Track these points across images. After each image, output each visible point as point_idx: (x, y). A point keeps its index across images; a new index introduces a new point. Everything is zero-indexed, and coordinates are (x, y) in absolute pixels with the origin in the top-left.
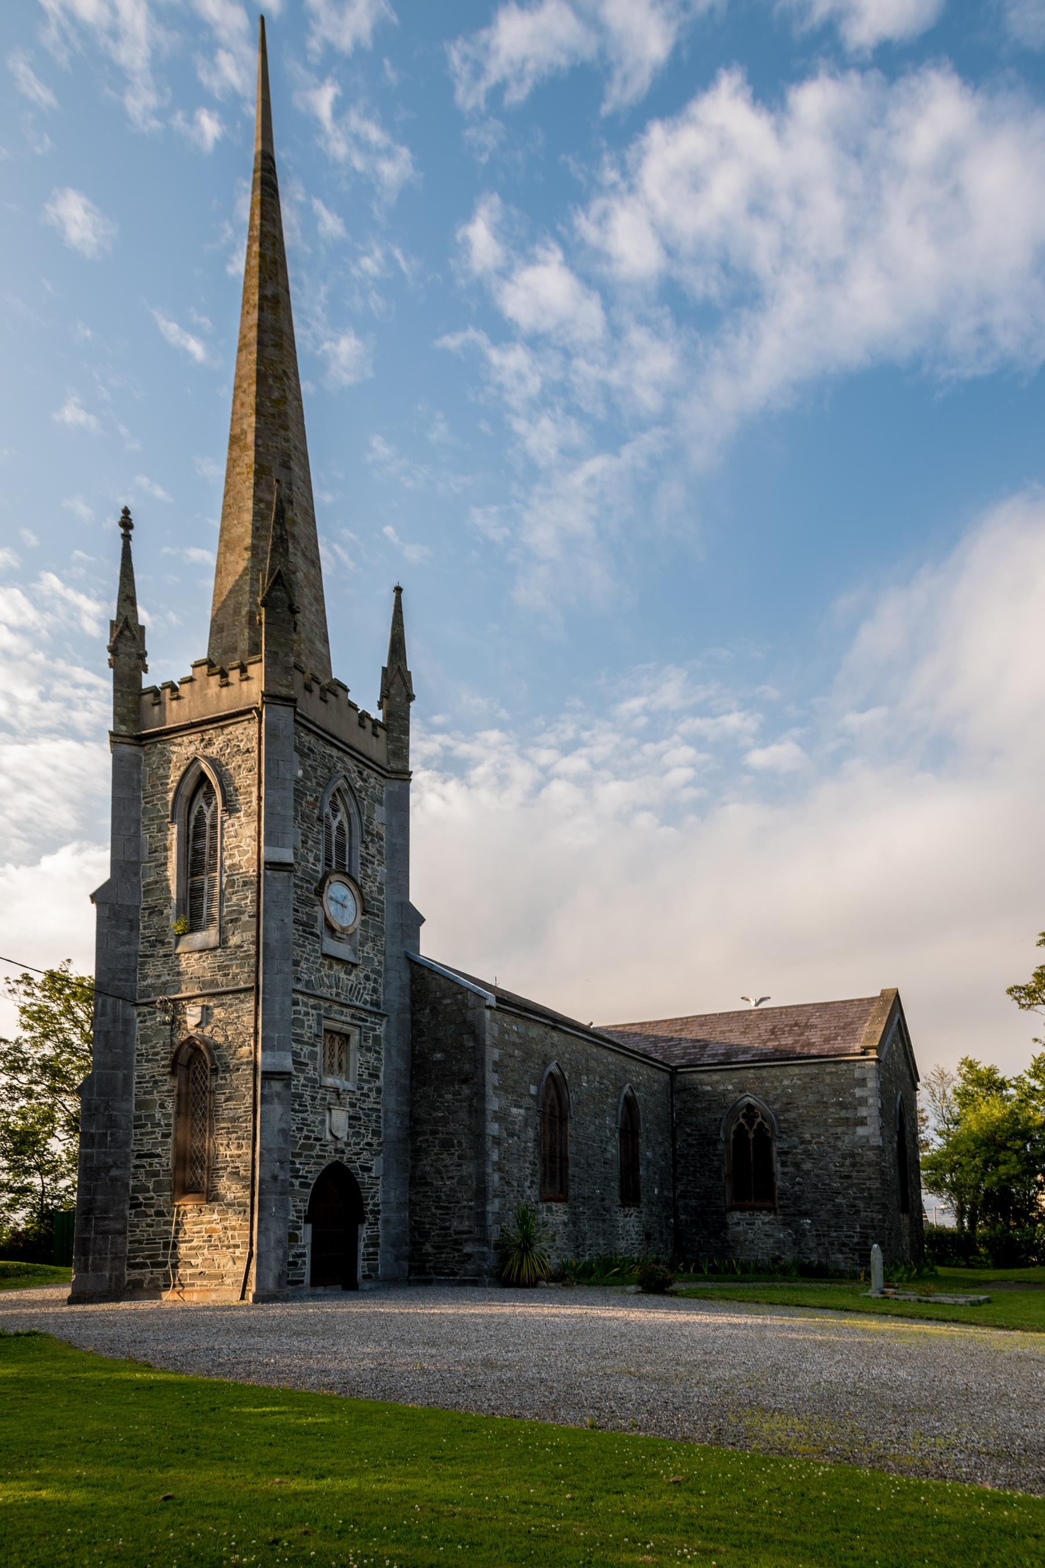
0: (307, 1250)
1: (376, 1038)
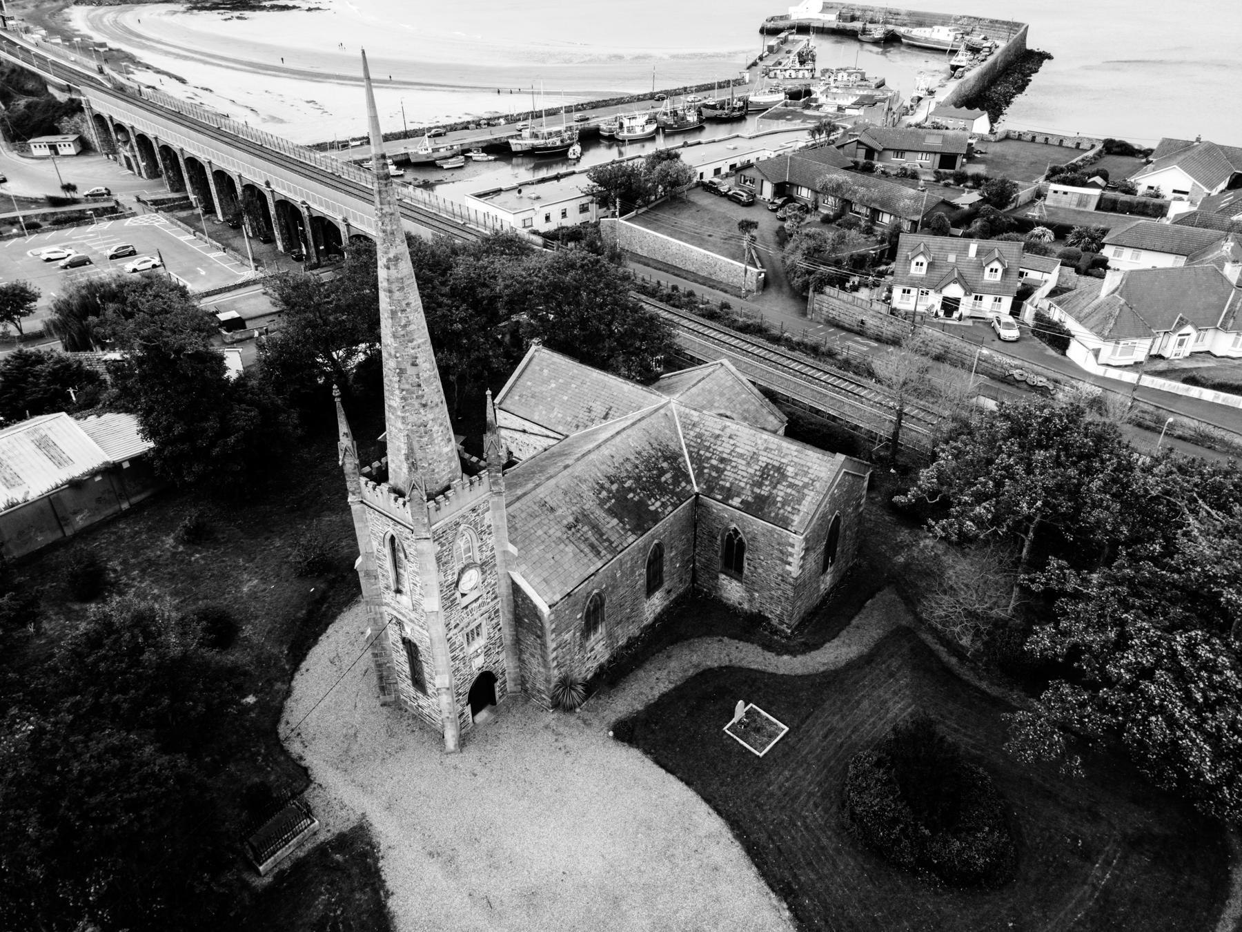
1: (497, 611)
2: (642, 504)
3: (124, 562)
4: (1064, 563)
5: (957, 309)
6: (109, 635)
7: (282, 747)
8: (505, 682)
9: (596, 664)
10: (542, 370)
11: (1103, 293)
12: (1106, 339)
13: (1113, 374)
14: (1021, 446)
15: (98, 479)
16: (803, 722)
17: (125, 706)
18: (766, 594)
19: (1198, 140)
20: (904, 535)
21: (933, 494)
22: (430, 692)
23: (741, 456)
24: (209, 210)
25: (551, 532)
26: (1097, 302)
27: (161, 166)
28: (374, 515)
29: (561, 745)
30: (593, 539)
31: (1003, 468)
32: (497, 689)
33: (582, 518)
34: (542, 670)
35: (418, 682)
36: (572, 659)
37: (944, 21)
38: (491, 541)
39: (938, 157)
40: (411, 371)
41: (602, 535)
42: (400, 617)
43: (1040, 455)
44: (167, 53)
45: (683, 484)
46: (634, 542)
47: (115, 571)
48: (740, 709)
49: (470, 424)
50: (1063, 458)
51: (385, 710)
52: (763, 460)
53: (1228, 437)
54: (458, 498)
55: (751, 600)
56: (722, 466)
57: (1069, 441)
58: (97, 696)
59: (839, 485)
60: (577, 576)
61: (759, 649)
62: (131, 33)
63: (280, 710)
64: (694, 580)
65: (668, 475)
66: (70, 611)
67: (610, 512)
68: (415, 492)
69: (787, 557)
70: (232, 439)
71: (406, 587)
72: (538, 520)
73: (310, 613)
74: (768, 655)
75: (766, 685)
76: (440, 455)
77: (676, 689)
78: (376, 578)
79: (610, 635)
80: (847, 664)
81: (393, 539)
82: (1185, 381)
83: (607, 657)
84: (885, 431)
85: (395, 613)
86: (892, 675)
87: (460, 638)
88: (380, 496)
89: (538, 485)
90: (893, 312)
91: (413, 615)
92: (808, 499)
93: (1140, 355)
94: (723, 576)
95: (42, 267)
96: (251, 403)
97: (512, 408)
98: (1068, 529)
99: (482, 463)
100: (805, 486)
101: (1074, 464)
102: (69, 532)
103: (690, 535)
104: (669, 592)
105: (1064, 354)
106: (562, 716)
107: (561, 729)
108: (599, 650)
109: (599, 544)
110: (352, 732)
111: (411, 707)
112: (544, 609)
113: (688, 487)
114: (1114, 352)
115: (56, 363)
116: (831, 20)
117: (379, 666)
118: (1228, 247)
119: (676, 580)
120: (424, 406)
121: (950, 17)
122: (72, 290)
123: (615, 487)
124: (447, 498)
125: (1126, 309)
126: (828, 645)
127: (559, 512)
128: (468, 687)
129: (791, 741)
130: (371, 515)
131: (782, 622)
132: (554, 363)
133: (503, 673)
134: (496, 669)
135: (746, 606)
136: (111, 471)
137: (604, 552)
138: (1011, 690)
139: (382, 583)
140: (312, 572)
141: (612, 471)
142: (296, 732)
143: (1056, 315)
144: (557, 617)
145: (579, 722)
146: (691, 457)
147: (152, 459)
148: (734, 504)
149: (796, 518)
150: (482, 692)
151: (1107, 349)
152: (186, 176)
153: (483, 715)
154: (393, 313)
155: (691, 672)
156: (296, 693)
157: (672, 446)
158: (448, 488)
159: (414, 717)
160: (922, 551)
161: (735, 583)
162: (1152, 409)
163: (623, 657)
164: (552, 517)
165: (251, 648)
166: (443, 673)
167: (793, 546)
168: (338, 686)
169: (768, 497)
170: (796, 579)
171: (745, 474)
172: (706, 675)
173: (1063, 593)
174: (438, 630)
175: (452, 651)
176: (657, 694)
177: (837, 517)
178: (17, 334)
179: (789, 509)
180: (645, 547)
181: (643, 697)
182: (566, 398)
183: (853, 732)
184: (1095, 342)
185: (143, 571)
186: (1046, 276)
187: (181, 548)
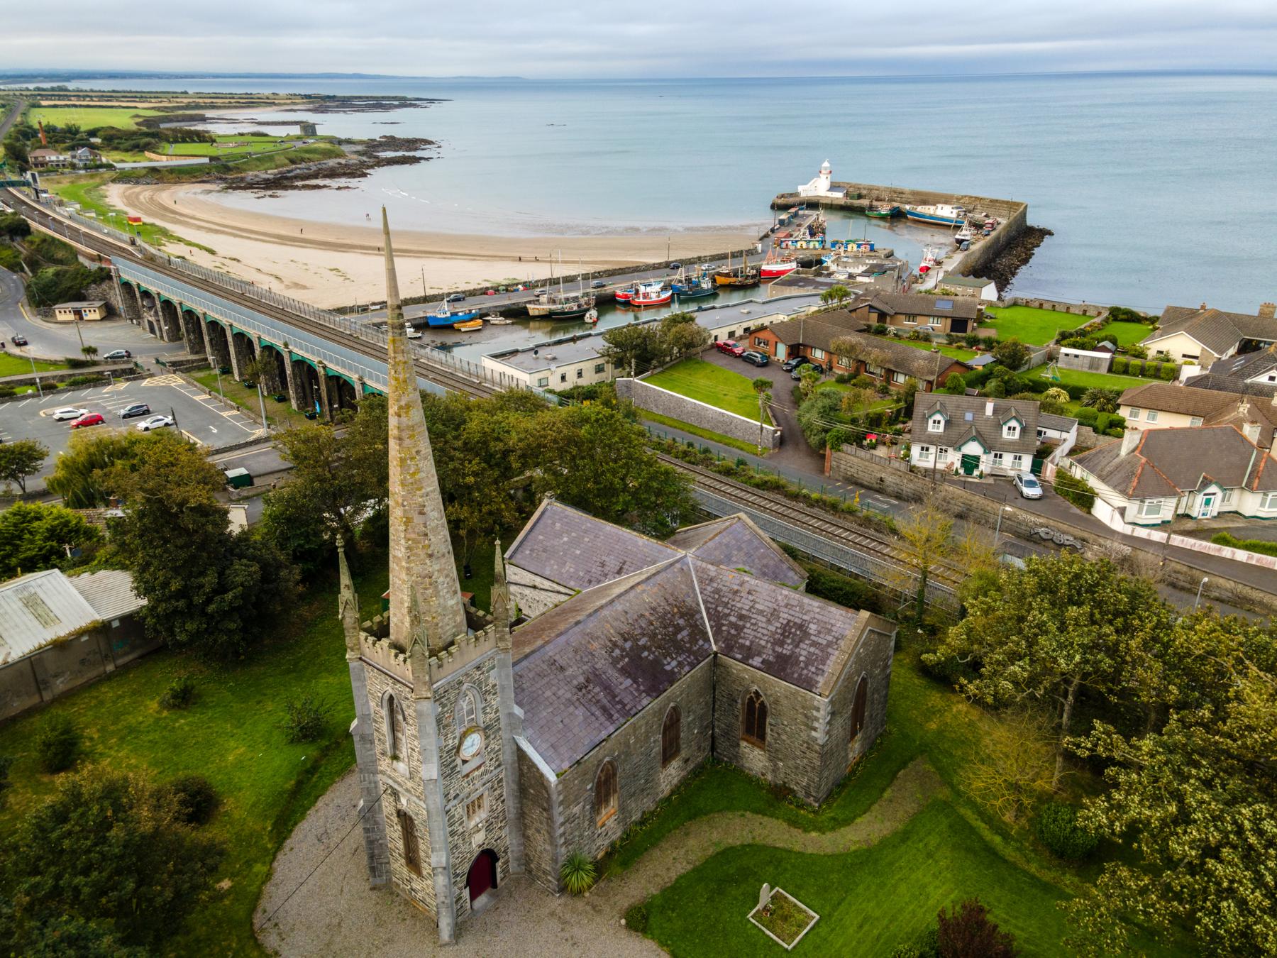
1: (501, 780)
2: (657, 663)
3: (103, 730)
4: (1111, 728)
5: (977, 466)
6: (76, 807)
7: (256, 939)
8: (507, 862)
9: (607, 842)
10: (554, 524)
11: (1124, 452)
12: (1130, 497)
13: (1142, 533)
14: (1053, 604)
15: (85, 638)
16: (835, 908)
17: (86, 890)
18: (791, 763)
19: (1203, 307)
20: (935, 698)
21: (963, 654)
22: (425, 873)
23: (761, 612)
24: (227, 371)
25: (561, 692)
26: (1117, 460)
27: (183, 329)
28: (376, 674)
29: (567, 935)
30: (605, 701)
31: (1038, 626)
32: (499, 870)
33: (594, 678)
34: (548, 848)
35: (412, 861)
36: (581, 836)
37: (947, 200)
38: (495, 702)
39: (949, 321)
40: (418, 519)
41: (614, 696)
42: (396, 786)
43: (1073, 611)
44: (199, 228)
45: (701, 642)
46: (650, 705)
47: (91, 739)
48: (765, 894)
49: (476, 574)
50: (1098, 616)
51: (374, 895)
52: (784, 615)
53: (1267, 599)
54: (462, 654)
55: (775, 770)
56: (741, 623)
57: (1106, 595)
58: (58, 877)
59: (864, 644)
60: (587, 742)
61: (785, 825)
62: (166, 209)
63: (258, 896)
64: (713, 749)
65: (685, 633)
66: (39, 783)
67: (624, 672)
68: (417, 647)
69: (811, 717)
70: (230, 595)
71: (404, 753)
72: (546, 680)
73: (299, 784)
74: (795, 831)
75: (793, 866)
76: (445, 608)
77: (695, 870)
78: (372, 742)
79: (622, 808)
80: (881, 842)
81: (391, 698)
82: (1216, 541)
83: (619, 834)
84: (910, 589)
85: (390, 782)
86: (930, 855)
87: (459, 810)
88: (379, 652)
89: (547, 643)
90: (913, 469)
91: (409, 784)
92: (833, 658)
93: (1167, 513)
94: (743, 744)
95: (54, 426)
96: (253, 558)
97: (522, 563)
98: (1110, 691)
99: (489, 617)
100: (829, 644)
101: (1110, 622)
102: (47, 696)
103: (709, 698)
104: (686, 761)
105: (1089, 513)
106: (570, 901)
107: (568, 917)
108: (610, 823)
109: (612, 707)
110: (335, 921)
111: (403, 890)
112: (552, 777)
113: (706, 646)
114: (1140, 511)
115: (55, 519)
116: (838, 196)
117: (371, 842)
118: (1244, 408)
119: (694, 748)
120: (431, 556)
121: (952, 196)
122: (81, 447)
123: (628, 645)
124: (450, 654)
125: (1147, 467)
126: (859, 820)
127: (569, 672)
128: (466, 867)
129: (823, 930)
130: (370, 673)
131: (808, 795)
132: (566, 517)
133: (505, 852)
134: (498, 847)
135: (769, 777)
136: (101, 630)
137: (616, 716)
138: (1064, 874)
139: (378, 749)
140: (305, 737)
141: (626, 628)
142: (273, 922)
143: (1078, 472)
144: (565, 788)
145: (588, 908)
146: (708, 613)
147: (144, 619)
148: (755, 664)
149: (821, 680)
150: (482, 873)
151: (1132, 507)
152: (206, 338)
153: (482, 900)
154: (402, 460)
155: (711, 851)
156: (277, 877)
157: (689, 601)
158: (452, 643)
159: (406, 903)
160: (955, 717)
161: (757, 751)
162: (1185, 569)
163: (636, 833)
164: (561, 677)
165: (231, 824)
166: (440, 850)
167: (818, 710)
168: (324, 867)
169: (790, 656)
170: (823, 746)
171: (765, 632)
172: (727, 854)
173: (1111, 761)
174: (437, 800)
175: (450, 826)
176: (673, 875)
177: (863, 679)
178: (20, 492)
179: (813, 669)
180: (661, 710)
181: (658, 879)
182: (578, 552)
183: (891, 922)
184: (1120, 501)
185: (122, 739)
186: (1065, 435)
187: (165, 713)
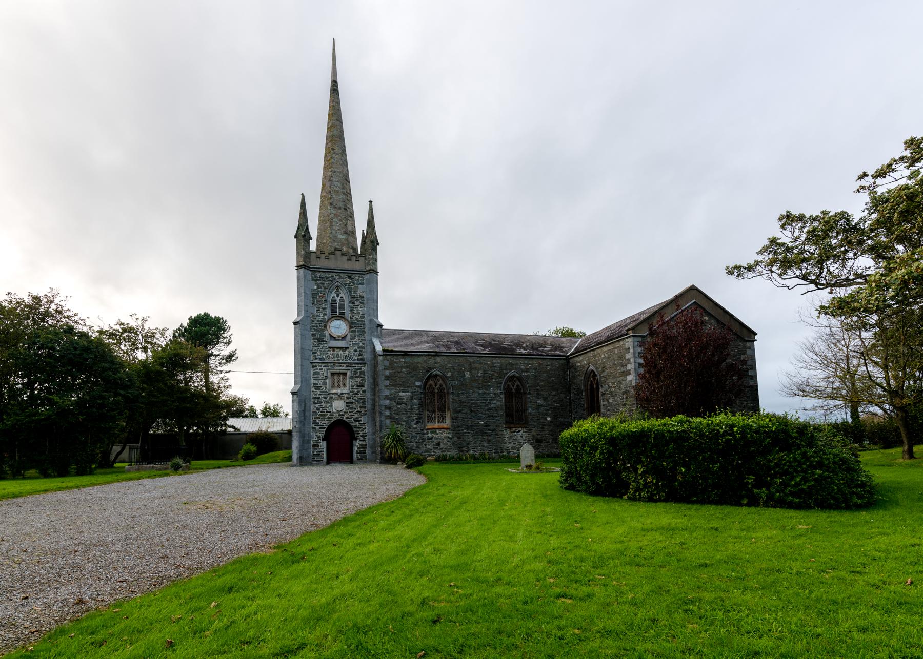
0: (325, 450)
32: (356, 449)
79: (456, 430)
133: (364, 436)
